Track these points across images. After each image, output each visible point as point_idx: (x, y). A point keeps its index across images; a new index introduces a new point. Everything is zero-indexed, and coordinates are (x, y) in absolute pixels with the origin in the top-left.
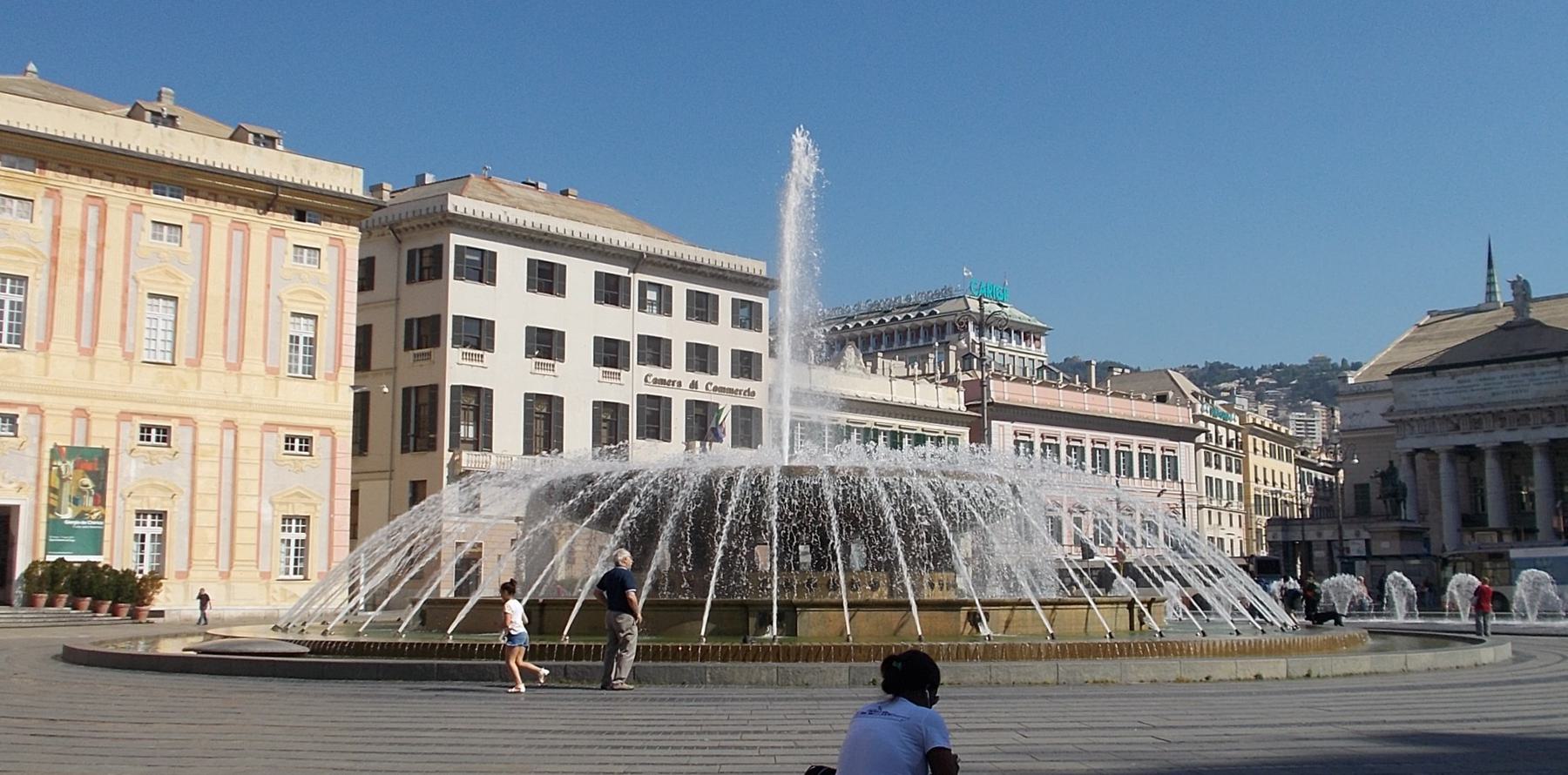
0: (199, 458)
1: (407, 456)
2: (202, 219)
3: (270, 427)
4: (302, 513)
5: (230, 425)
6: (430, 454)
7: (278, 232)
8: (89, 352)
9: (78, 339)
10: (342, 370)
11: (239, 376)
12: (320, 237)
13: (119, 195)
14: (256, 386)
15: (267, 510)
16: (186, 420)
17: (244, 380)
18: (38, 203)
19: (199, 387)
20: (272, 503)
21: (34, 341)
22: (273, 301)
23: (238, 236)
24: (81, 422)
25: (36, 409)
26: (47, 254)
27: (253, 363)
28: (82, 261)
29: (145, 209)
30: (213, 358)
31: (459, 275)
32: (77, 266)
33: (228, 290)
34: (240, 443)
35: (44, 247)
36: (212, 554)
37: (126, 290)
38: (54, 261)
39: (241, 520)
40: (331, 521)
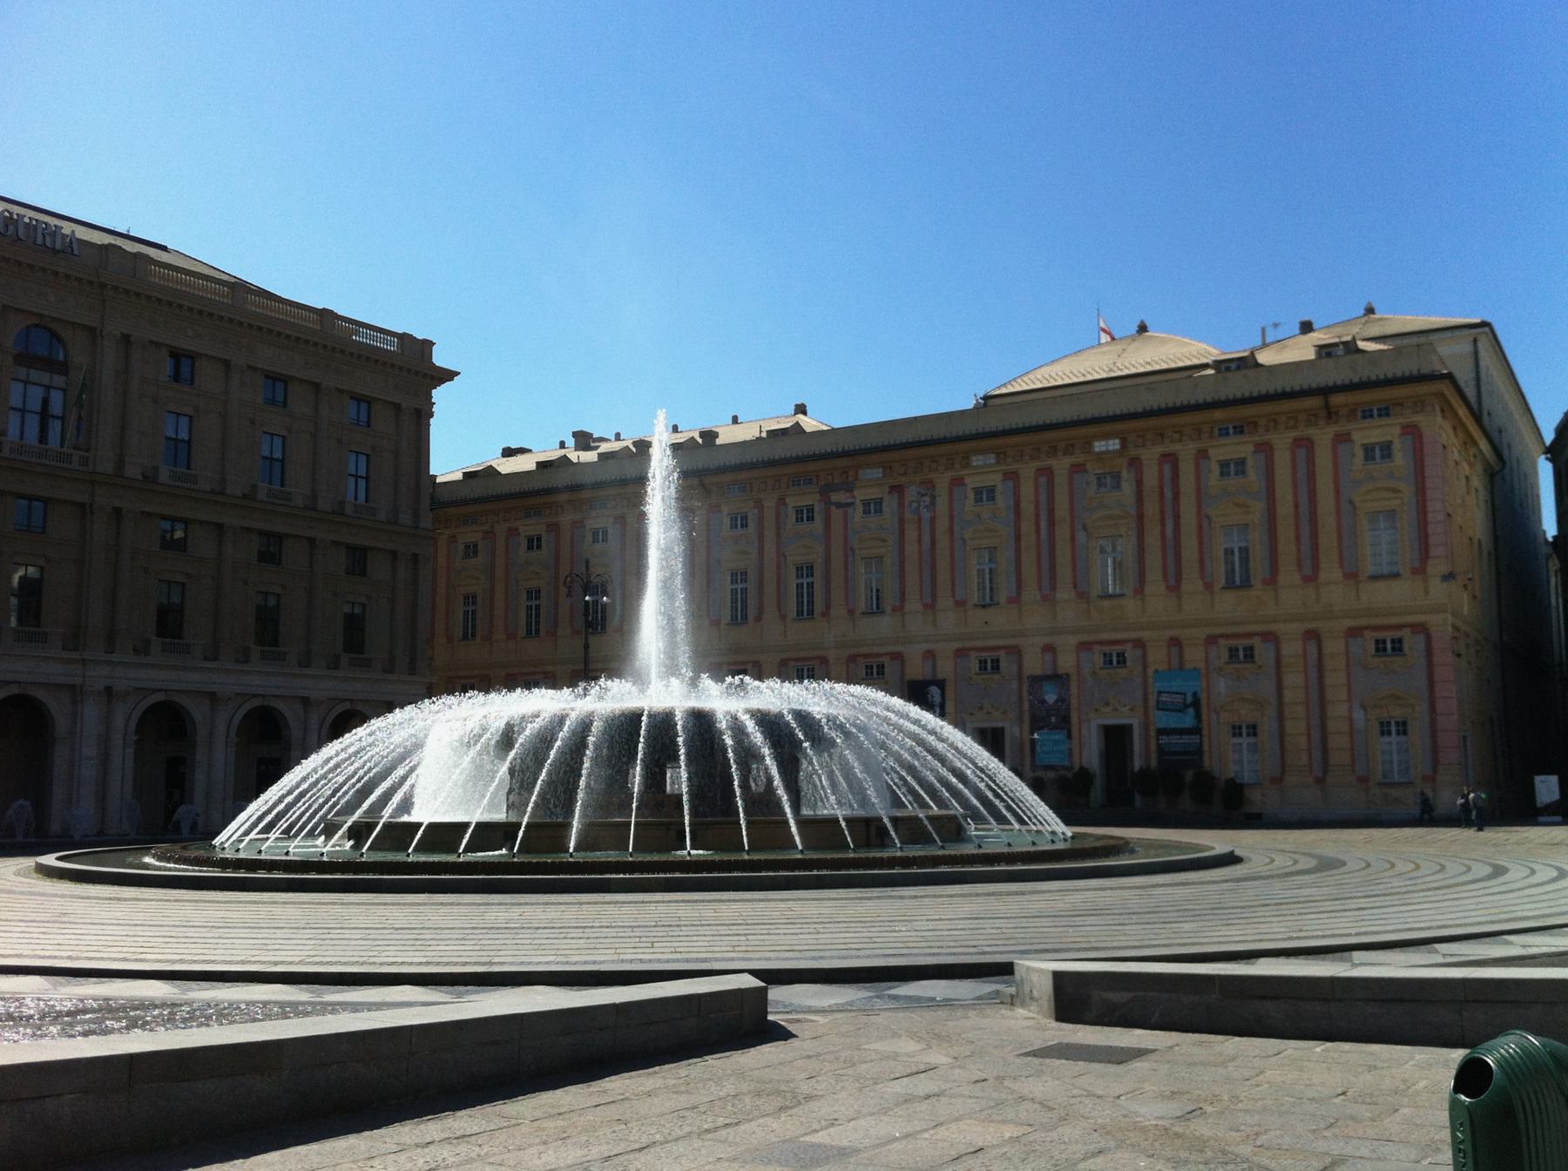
3: (1354, 632)
4: (1397, 713)
5: (1313, 635)
7: (1342, 438)
8: (1175, 588)
10: (1430, 562)
13: (1186, 451)
14: (1335, 592)
15: (1358, 715)
18: (1124, 474)
20: (1364, 707)
23: (1301, 453)
25: (1139, 644)
27: (1331, 571)
28: (1162, 512)
29: (1212, 452)
30: (1289, 575)
35: (1132, 511)
36: (1304, 758)
37: (1200, 528)
38: (1140, 517)
39: (1332, 726)
40: (1433, 723)
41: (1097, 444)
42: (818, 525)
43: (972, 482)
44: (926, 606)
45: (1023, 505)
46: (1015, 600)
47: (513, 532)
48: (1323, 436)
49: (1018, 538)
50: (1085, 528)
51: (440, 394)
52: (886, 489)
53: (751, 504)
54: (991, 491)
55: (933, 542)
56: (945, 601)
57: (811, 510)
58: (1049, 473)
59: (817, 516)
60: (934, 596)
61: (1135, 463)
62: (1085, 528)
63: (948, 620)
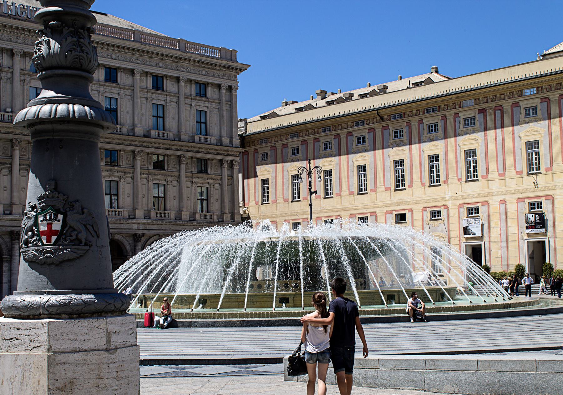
43: (523, 105)
44: (500, 175)
47: (285, 146)
49: (550, 134)
51: (240, 77)
53: (405, 124)
54: (535, 109)
55: (503, 140)
56: (511, 172)
57: (436, 126)
59: (440, 128)
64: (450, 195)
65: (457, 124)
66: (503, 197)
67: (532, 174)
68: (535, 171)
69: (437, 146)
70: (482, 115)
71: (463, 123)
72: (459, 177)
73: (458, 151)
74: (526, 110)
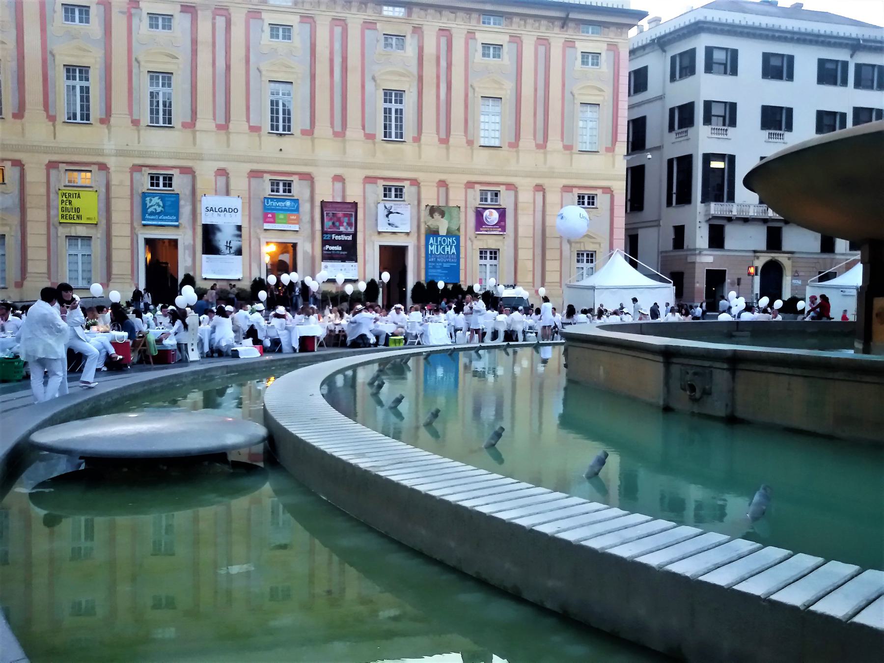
0: (519, 212)
1: (670, 209)
2: (516, 40)
4: (590, 248)
5: (540, 188)
6: (687, 208)
7: (569, 44)
9: (438, 132)
10: (618, 144)
11: (545, 154)
12: (599, 44)
14: (556, 159)
16: (510, 186)
17: (549, 156)
19: (518, 161)
20: (569, 242)
21: (411, 135)
22: (568, 95)
23: (542, 49)
24: (442, 190)
25: (415, 182)
26: (416, 74)
27: (555, 143)
28: (438, 77)
29: (478, 35)
30: (527, 141)
31: (709, 69)
32: (435, 81)
33: (536, 90)
34: (548, 200)
35: (414, 69)
36: (530, 278)
37: (466, 96)
38: (420, 79)
41: (385, 8)
42: (95, 25)
44: (219, 127)
45: (318, 49)
46: (309, 132)
48: (557, 38)
49: (313, 77)
50: (374, 79)
52: (179, 8)
54: (287, 28)
55: (228, 68)
56: (238, 123)
58: (341, 22)
60: (228, 119)
61: (417, 30)
62: (374, 79)
63: (241, 141)
64: (113, 147)
65: (135, 21)
66: (222, 165)
67: (281, 135)
68: (281, 131)
69: (85, 50)
70: (188, 16)
71: (146, 21)
72: (135, 117)
73: (135, 71)
74: (272, 29)
